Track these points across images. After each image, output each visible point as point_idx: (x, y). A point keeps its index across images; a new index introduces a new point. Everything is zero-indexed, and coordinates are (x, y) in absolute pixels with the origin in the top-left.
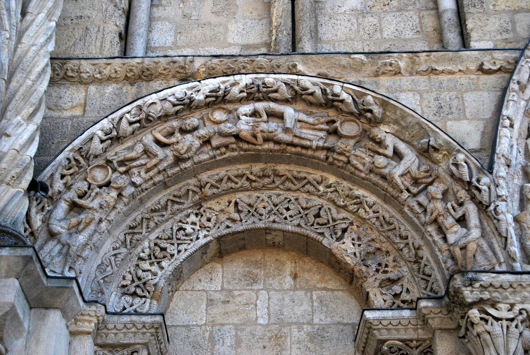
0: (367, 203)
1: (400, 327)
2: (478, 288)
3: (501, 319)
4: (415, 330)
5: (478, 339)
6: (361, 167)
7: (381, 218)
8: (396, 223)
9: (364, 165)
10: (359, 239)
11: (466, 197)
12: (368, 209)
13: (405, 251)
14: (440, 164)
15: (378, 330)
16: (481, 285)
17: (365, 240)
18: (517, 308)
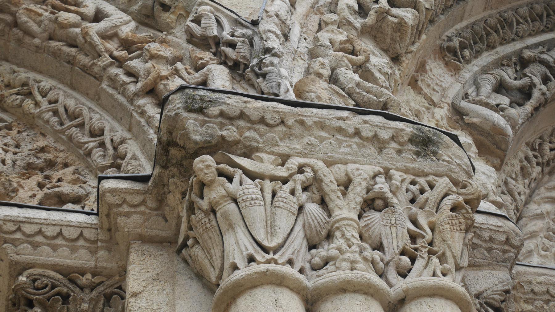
0: (39, 89)
1: (59, 241)
2: (216, 117)
3: (262, 177)
4: (94, 252)
5: (212, 216)
6: (35, 28)
7: (62, 110)
8: (85, 112)
9: (39, 24)
10: (18, 146)
11: (211, 59)
12: (39, 98)
13: (97, 153)
14: (172, 31)
15: (14, 242)
16: (222, 114)
17: (27, 148)
18: (294, 162)
